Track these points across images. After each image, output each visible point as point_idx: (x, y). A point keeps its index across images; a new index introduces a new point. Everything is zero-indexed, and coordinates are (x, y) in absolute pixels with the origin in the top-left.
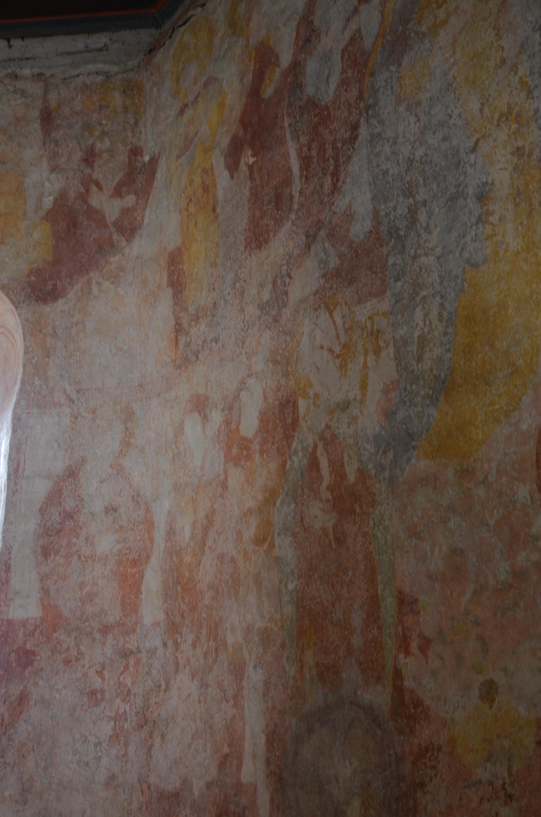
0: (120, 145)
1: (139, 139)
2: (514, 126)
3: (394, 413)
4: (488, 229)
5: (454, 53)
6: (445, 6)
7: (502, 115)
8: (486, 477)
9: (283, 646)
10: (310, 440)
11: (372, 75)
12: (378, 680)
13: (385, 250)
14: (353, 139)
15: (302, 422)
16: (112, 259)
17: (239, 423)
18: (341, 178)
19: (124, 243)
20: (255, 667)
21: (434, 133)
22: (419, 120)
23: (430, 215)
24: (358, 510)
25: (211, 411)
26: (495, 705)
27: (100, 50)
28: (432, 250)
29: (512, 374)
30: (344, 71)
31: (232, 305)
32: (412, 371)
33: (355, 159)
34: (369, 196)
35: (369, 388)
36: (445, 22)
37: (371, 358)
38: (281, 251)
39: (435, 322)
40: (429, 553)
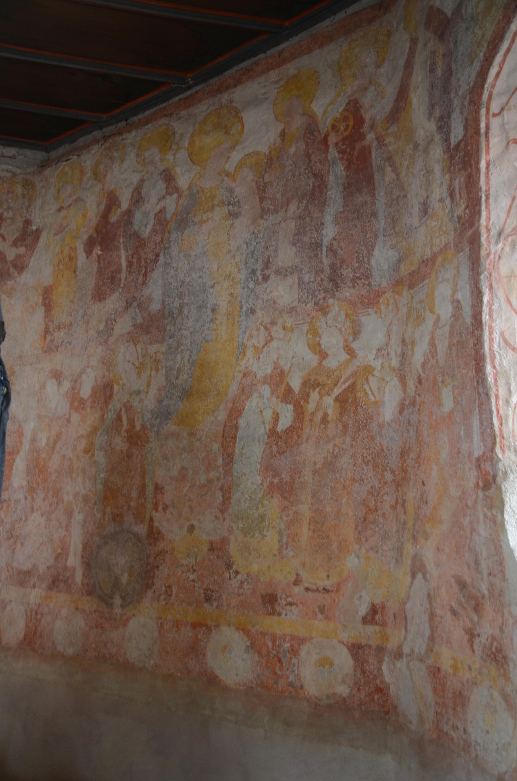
0: (18, 216)
1: (31, 216)
2: (231, 282)
3: (162, 401)
4: (215, 326)
5: (209, 238)
6: (207, 214)
7: (226, 276)
8: (201, 438)
9: (95, 503)
10: (118, 406)
11: (169, 233)
12: (142, 522)
13: (166, 321)
14: (156, 261)
15: (115, 396)
16: (9, 283)
17: (80, 390)
18: (148, 279)
19: (16, 274)
20: (79, 513)
21: (196, 273)
22: (189, 264)
23: (189, 311)
24: (140, 443)
25: (64, 380)
26: (193, 535)
27: (10, 157)
28: (188, 328)
29: (217, 394)
30: (154, 225)
31: (81, 327)
32: (173, 383)
33: (156, 271)
34: (161, 292)
35: (151, 386)
36: (206, 222)
37: (153, 373)
38: (112, 306)
39: (186, 363)
40: (172, 468)
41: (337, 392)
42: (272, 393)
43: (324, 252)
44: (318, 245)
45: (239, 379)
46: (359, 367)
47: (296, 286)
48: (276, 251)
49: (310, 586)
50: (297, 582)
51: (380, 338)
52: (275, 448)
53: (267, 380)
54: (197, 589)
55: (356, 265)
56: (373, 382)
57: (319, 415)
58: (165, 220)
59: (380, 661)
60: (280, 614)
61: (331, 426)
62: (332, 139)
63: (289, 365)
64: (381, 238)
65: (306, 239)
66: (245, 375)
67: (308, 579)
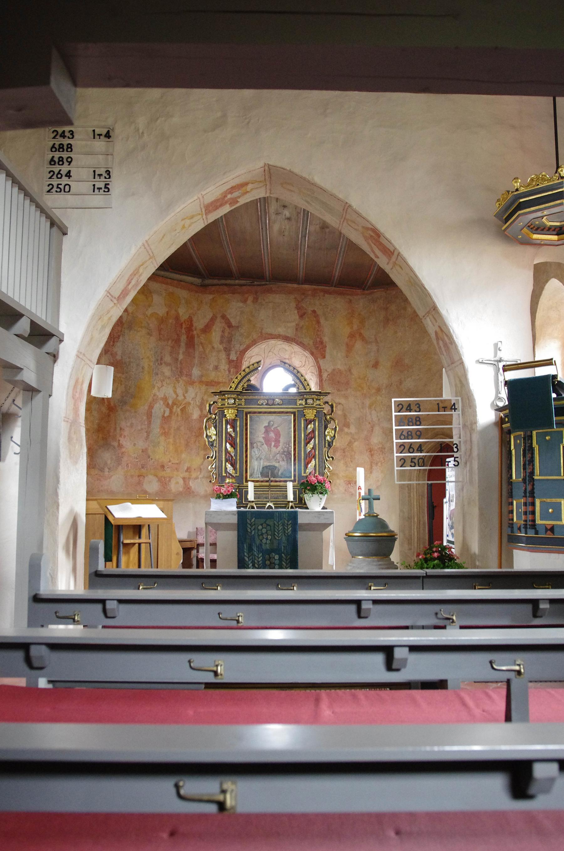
3: (124, 397)
9: (93, 432)
23: (133, 365)
36: (139, 331)
41: (181, 407)
42: (163, 404)
43: (179, 363)
44: (177, 359)
47: (170, 370)
48: (165, 355)
50: (170, 461)
51: (193, 395)
52: (164, 421)
54: (138, 464)
56: (191, 407)
58: (122, 322)
59: (189, 481)
61: (179, 417)
62: (184, 326)
64: (195, 366)
65: (174, 355)
66: (154, 395)
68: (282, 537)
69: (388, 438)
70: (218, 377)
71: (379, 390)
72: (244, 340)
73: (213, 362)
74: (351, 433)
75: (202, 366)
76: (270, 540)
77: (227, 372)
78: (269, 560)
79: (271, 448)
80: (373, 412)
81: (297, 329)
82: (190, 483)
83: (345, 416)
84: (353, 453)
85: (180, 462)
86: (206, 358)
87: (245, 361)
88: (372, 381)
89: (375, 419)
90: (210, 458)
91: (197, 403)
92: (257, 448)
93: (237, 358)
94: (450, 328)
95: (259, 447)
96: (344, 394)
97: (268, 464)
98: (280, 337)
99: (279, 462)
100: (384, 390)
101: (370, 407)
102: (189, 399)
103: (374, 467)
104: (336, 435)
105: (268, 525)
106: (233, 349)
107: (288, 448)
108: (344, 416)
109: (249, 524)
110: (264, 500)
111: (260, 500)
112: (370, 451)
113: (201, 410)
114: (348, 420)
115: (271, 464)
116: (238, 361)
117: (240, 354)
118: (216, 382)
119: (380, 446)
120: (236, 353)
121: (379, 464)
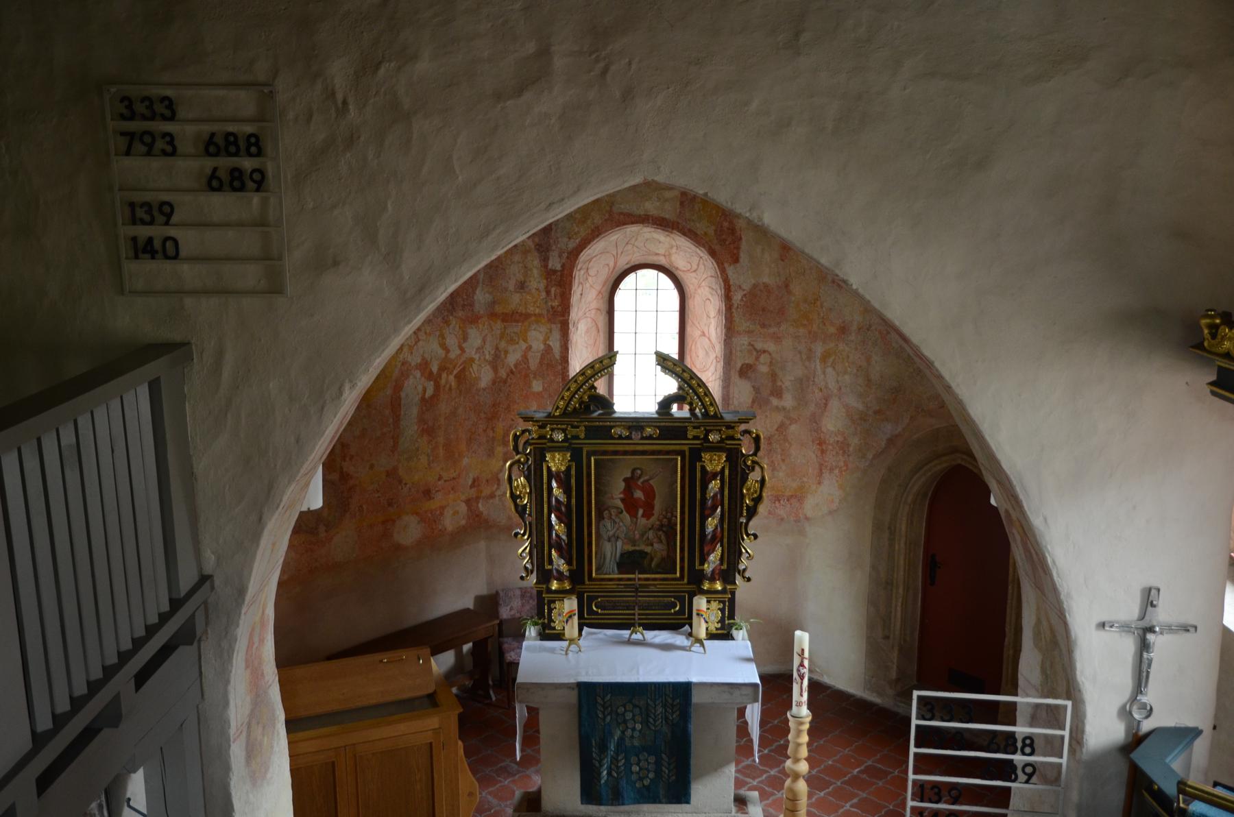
41: (455, 372)
42: (422, 375)
45: (399, 366)
46: (466, 358)
49: (447, 479)
50: (439, 479)
51: (479, 342)
52: (424, 408)
53: (418, 367)
55: (465, 297)
56: (475, 367)
57: (448, 386)
59: (478, 503)
60: (434, 498)
63: (430, 357)
66: (403, 364)
67: (445, 475)
68: (662, 726)
69: (856, 429)
70: (525, 303)
71: (843, 330)
72: (576, 229)
73: (514, 275)
74: (784, 409)
75: (493, 284)
76: (640, 731)
77: (544, 294)
78: (638, 764)
79: (637, 519)
80: (829, 370)
81: (682, 203)
82: (480, 505)
83: (774, 376)
84: (787, 444)
85: (459, 475)
86: (501, 266)
87: (580, 270)
88: (831, 309)
89: (832, 385)
90: (519, 536)
91: (487, 357)
92: (610, 518)
93: (563, 266)
94: (1047, 555)
95: (613, 517)
96: (774, 333)
97: (633, 548)
98: (648, 220)
99: (652, 545)
100: (853, 334)
101: (824, 359)
102: (471, 352)
103: (826, 475)
104: (764, 494)
105: (635, 706)
106: (554, 247)
107: (670, 520)
108: (772, 376)
109: (601, 704)
110: (625, 612)
111: (617, 612)
112: (820, 444)
113: (495, 369)
114: (779, 383)
115: (637, 548)
116: (566, 272)
117: (568, 258)
118: (521, 314)
119: (840, 438)
120: (560, 256)
121: (837, 471)
